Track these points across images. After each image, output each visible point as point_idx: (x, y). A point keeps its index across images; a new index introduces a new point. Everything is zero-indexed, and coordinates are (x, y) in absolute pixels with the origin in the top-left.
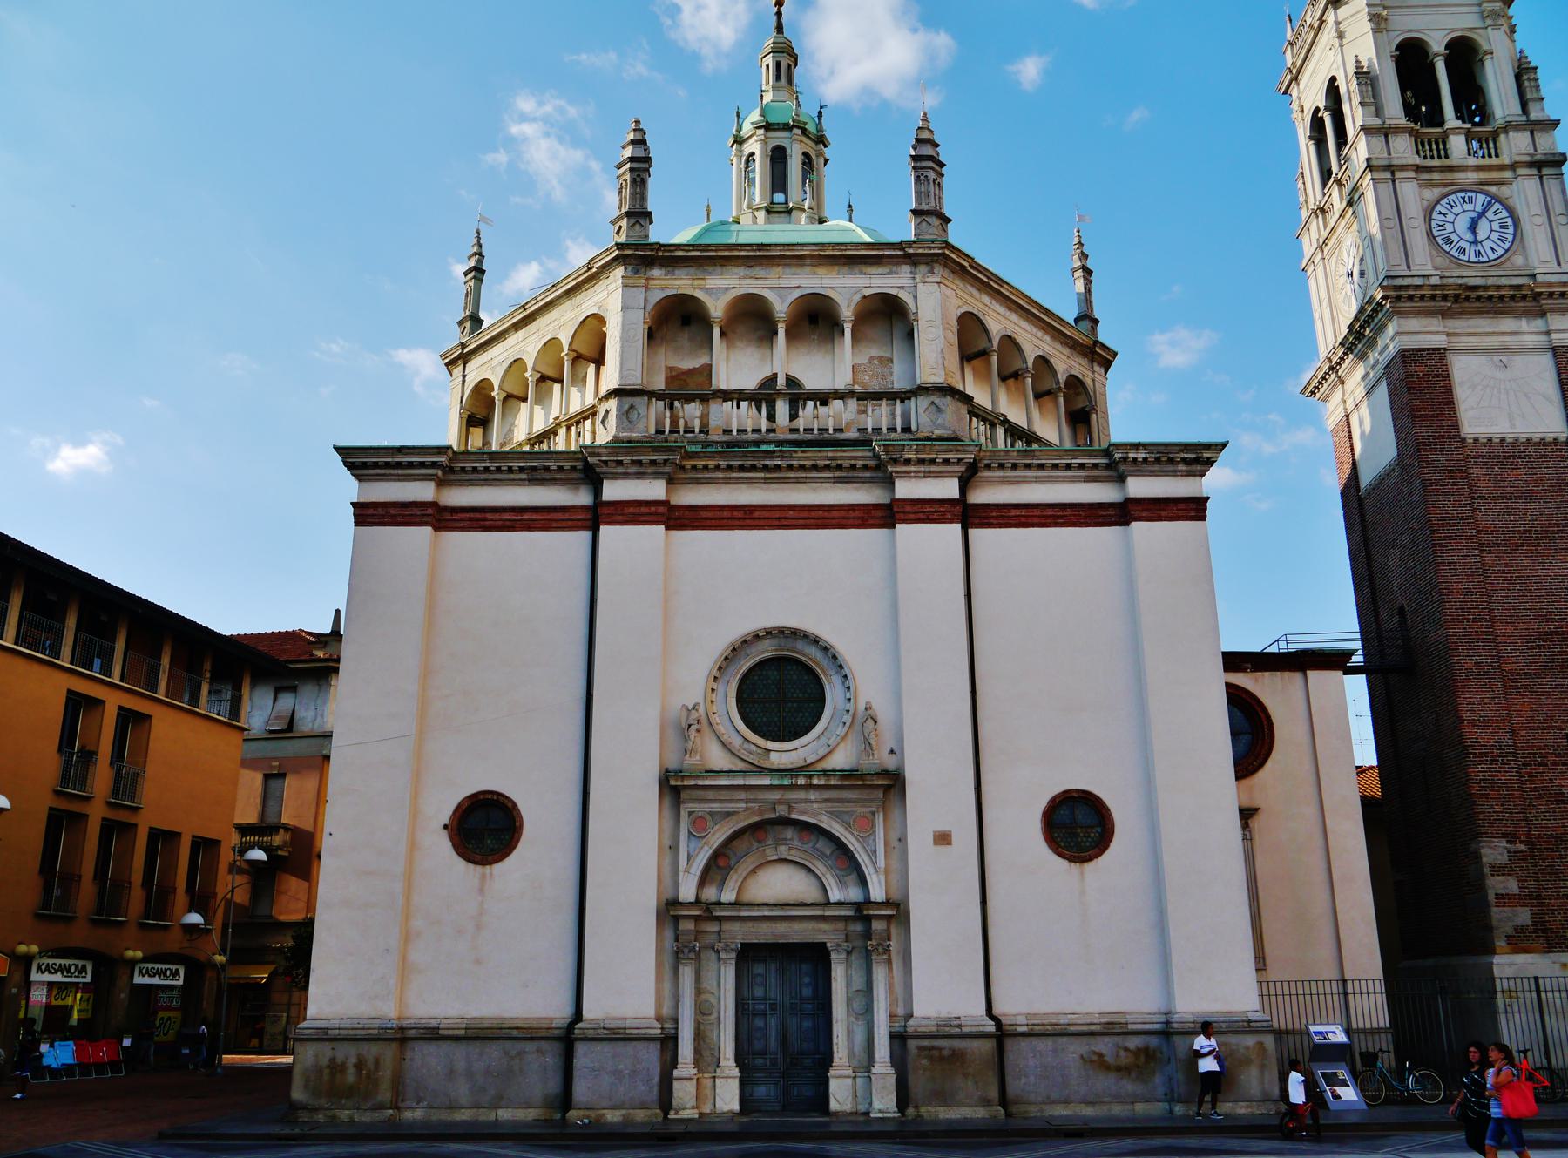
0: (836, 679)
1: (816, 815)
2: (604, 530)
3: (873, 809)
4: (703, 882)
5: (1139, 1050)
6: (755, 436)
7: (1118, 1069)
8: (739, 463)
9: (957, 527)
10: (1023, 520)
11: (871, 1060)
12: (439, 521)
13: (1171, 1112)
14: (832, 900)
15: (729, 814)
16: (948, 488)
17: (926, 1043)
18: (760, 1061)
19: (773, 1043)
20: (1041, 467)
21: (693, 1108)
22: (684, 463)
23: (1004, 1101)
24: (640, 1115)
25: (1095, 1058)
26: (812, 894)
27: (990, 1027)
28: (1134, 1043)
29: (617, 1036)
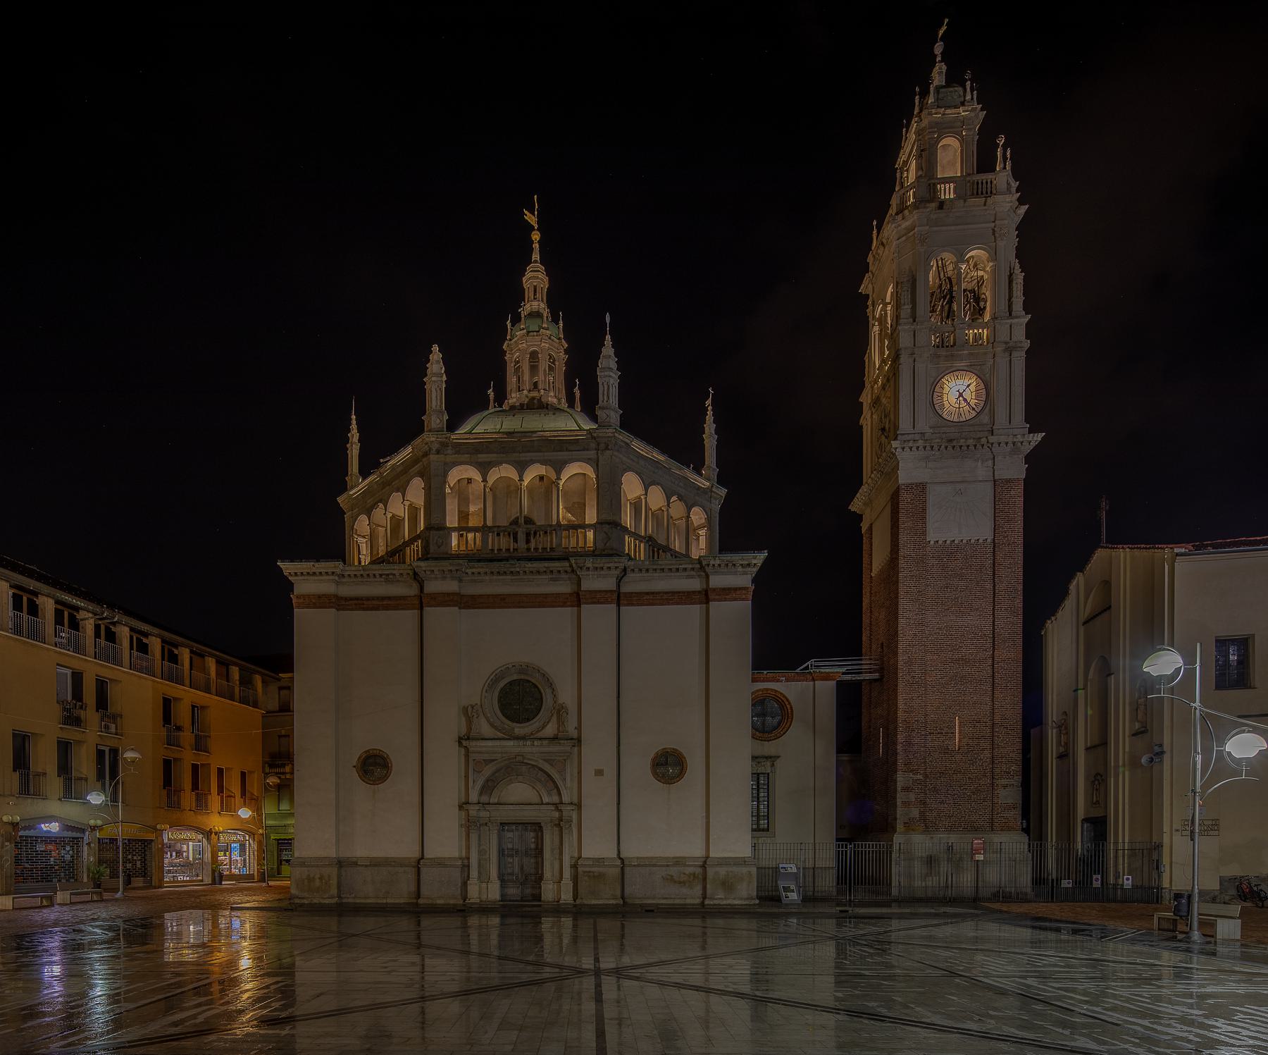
0: (548, 691)
1: (536, 761)
2: (426, 609)
3: (565, 758)
4: (481, 794)
5: (691, 874)
6: (507, 555)
7: (680, 883)
8: (497, 570)
9: (614, 606)
10: (651, 601)
11: (561, 878)
12: (339, 605)
13: (703, 902)
14: (544, 802)
15: (493, 760)
16: (608, 584)
17: (588, 869)
18: (510, 877)
19: (517, 870)
20: (663, 570)
21: (477, 898)
22: (467, 571)
23: (623, 897)
24: (452, 902)
25: (669, 877)
26: (537, 800)
27: (619, 862)
28: (689, 870)
29: (440, 863)
